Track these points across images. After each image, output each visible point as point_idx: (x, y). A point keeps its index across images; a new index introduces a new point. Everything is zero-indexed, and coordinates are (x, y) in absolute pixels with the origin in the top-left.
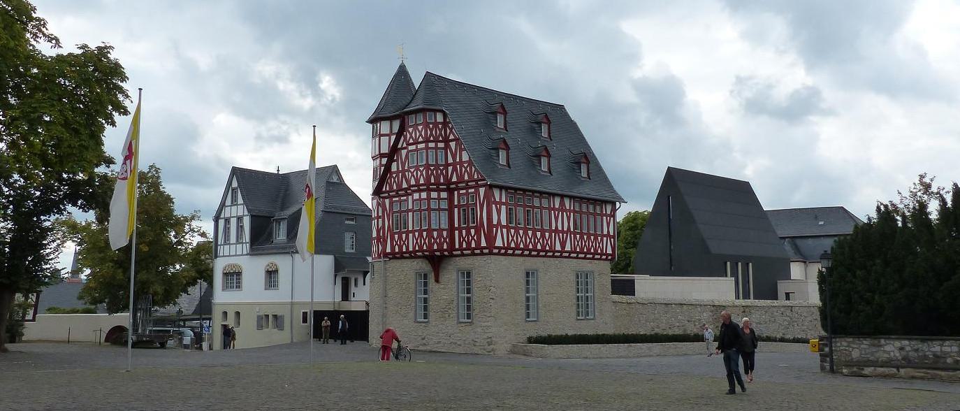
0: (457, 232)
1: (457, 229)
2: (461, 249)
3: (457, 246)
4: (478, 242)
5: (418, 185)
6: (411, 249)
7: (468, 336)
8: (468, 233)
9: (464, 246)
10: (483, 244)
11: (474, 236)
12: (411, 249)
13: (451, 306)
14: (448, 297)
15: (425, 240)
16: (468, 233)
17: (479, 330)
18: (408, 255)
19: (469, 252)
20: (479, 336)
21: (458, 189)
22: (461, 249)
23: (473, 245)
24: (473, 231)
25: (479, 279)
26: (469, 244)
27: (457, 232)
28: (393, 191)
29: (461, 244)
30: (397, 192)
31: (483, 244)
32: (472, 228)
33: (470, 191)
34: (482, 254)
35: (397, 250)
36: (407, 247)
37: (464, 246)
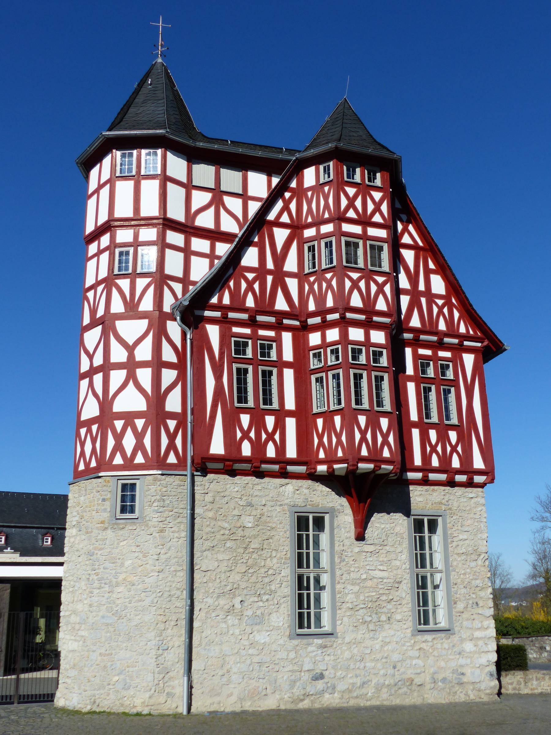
0: (416, 433)
1: (415, 425)
2: (426, 468)
3: (418, 461)
4: (467, 458)
5: (322, 312)
6: (291, 452)
7: (442, 664)
8: (443, 438)
9: (435, 462)
10: (478, 463)
11: (457, 444)
12: (291, 452)
13: (395, 595)
14: (384, 574)
15: (385, 437)
16: (443, 438)
17: (469, 646)
18: (276, 467)
19: (443, 477)
20: (469, 661)
21: (416, 343)
22: (426, 468)
23: (456, 463)
24: (453, 436)
25: (461, 537)
26: (445, 460)
27: (416, 433)
28: (245, 310)
29: (426, 458)
30: (253, 313)
31: (478, 463)
32: (452, 427)
33: (441, 354)
34: (470, 484)
35: (246, 450)
36: (281, 449)
37: (435, 462)
